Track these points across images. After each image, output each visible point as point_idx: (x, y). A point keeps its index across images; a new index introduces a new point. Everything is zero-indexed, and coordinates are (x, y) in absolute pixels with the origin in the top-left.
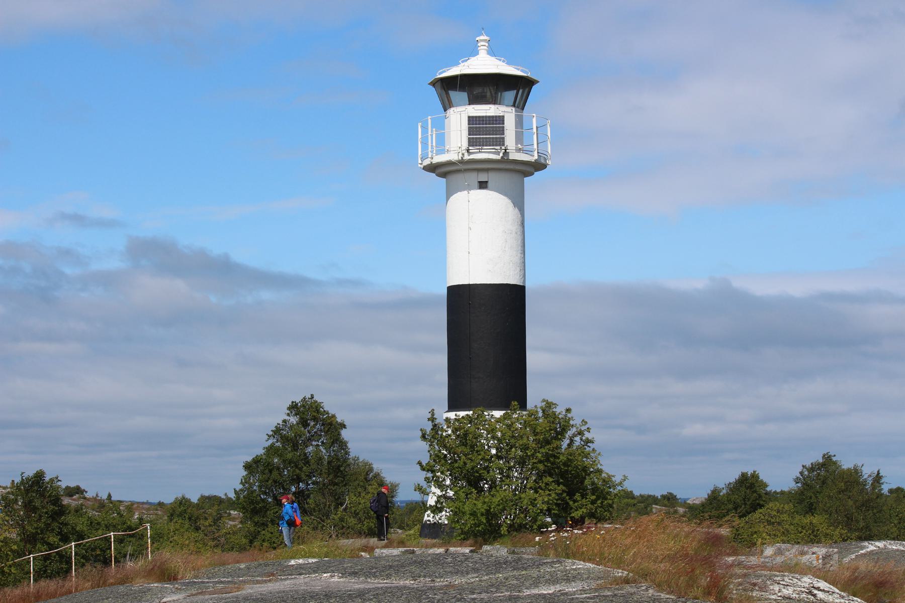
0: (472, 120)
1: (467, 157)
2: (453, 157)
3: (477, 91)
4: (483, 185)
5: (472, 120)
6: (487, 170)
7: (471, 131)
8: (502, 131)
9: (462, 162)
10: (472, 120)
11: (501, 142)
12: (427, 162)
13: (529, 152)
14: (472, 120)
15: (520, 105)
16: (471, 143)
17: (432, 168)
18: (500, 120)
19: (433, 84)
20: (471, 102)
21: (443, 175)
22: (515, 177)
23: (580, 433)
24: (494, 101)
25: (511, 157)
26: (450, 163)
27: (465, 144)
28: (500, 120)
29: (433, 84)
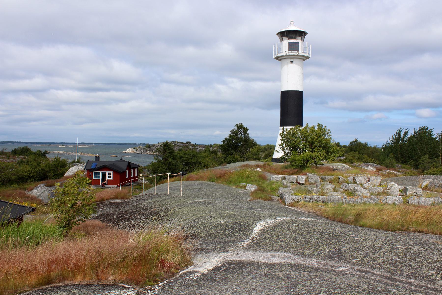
0: (289, 43)
1: (288, 54)
2: (284, 54)
3: (290, 35)
4: (292, 62)
5: (289, 43)
6: (293, 58)
7: (289, 47)
8: (298, 46)
9: (286, 55)
10: (289, 43)
11: (298, 50)
12: (276, 56)
13: (306, 53)
14: (289, 43)
15: (303, 40)
16: (289, 50)
17: (277, 58)
18: (298, 43)
19: (278, 34)
20: (288, 39)
21: (280, 60)
22: (302, 60)
23: (328, 133)
24: (295, 39)
25: (300, 54)
26: (283, 56)
27: (287, 50)
28: (298, 43)
29: (278, 34)
